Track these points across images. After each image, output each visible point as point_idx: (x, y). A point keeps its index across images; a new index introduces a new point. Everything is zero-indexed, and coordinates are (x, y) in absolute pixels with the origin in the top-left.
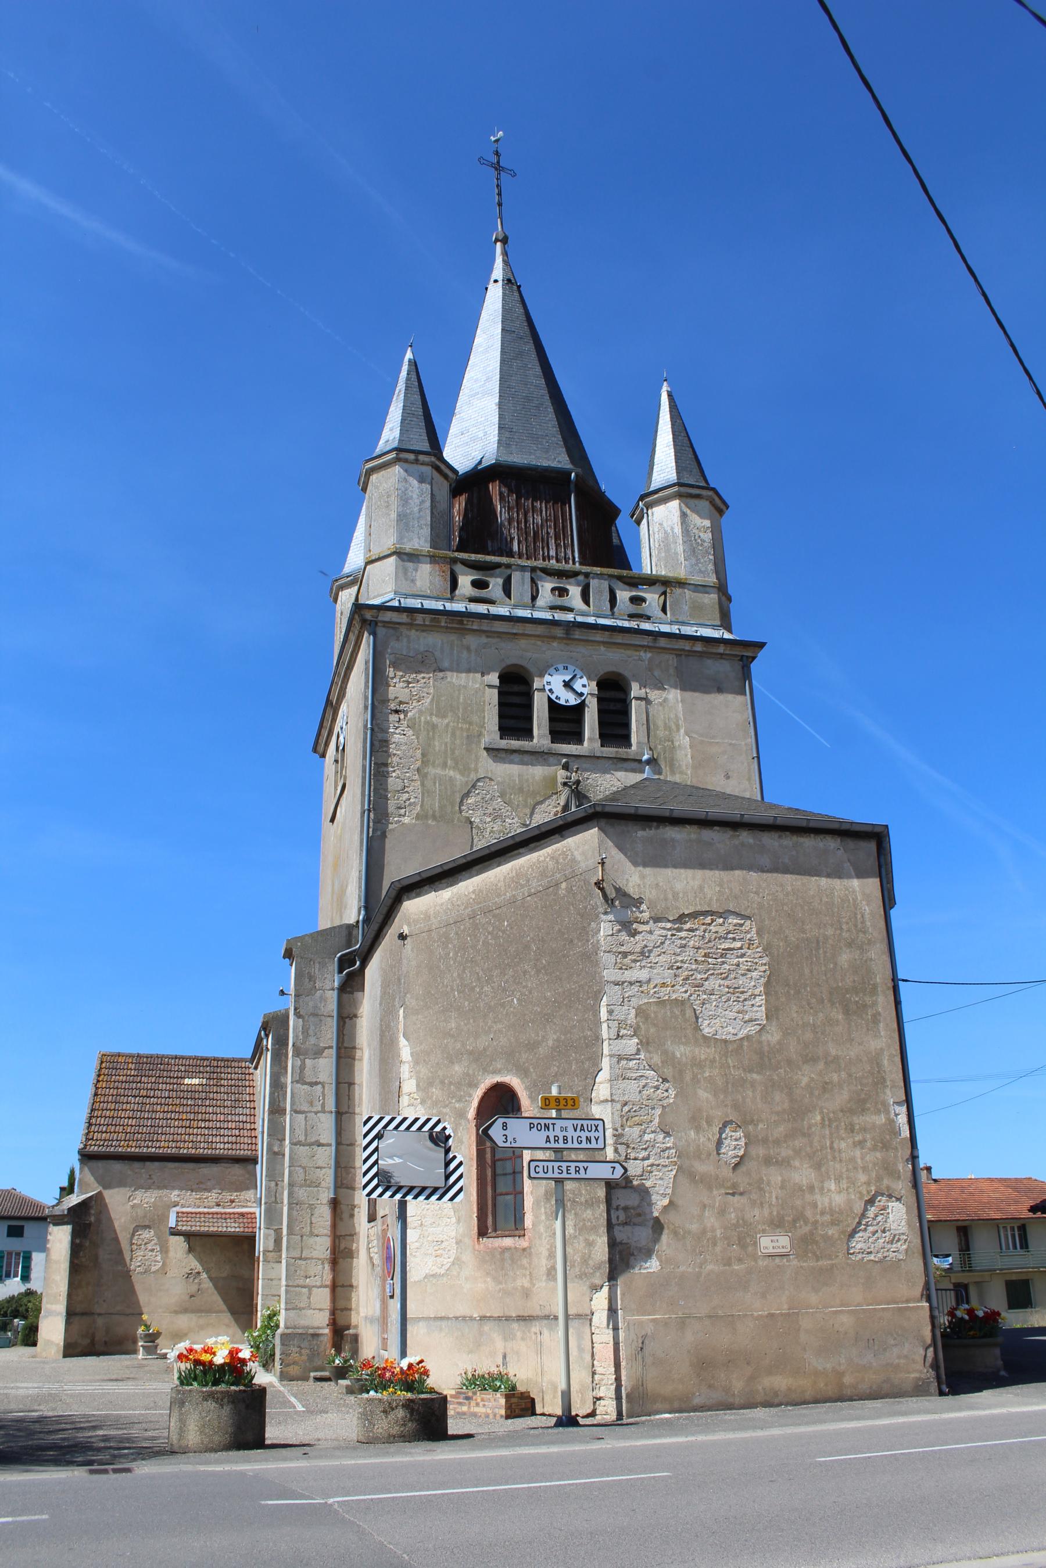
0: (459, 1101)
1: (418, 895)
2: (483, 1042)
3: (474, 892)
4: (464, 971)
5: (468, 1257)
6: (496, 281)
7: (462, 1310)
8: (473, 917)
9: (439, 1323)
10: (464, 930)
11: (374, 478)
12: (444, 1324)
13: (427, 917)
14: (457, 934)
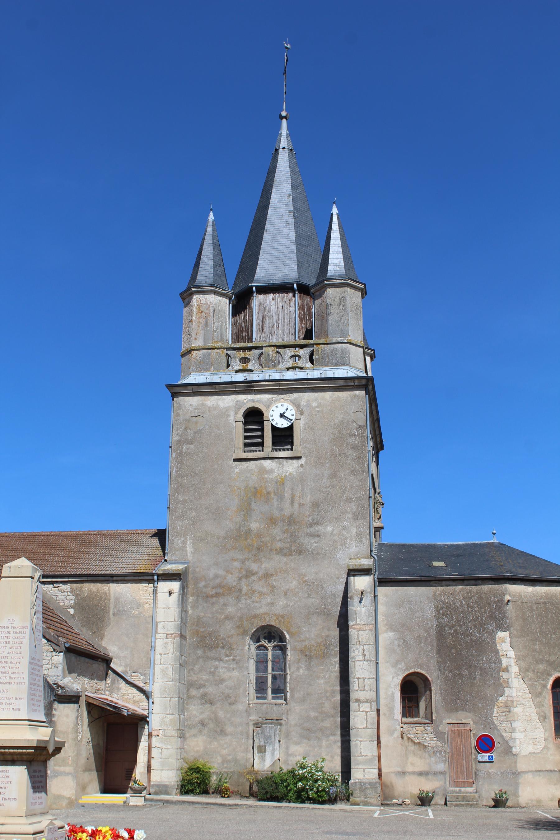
0: (543, 680)
1: (514, 584)
2: (553, 658)
3: (545, 593)
4: (542, 625)
5: (551, 745)
6: (284, 148)
7: (549, 767)
8: (545, 603)
9: (538, 773)
10: (541, 608)
11: (348, 289)
12: (541, 773)
13: (520, 596)
14: (537, 608)
